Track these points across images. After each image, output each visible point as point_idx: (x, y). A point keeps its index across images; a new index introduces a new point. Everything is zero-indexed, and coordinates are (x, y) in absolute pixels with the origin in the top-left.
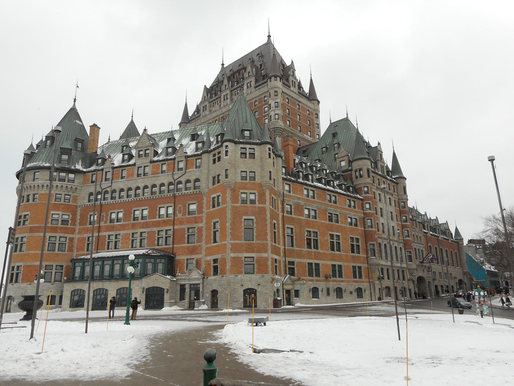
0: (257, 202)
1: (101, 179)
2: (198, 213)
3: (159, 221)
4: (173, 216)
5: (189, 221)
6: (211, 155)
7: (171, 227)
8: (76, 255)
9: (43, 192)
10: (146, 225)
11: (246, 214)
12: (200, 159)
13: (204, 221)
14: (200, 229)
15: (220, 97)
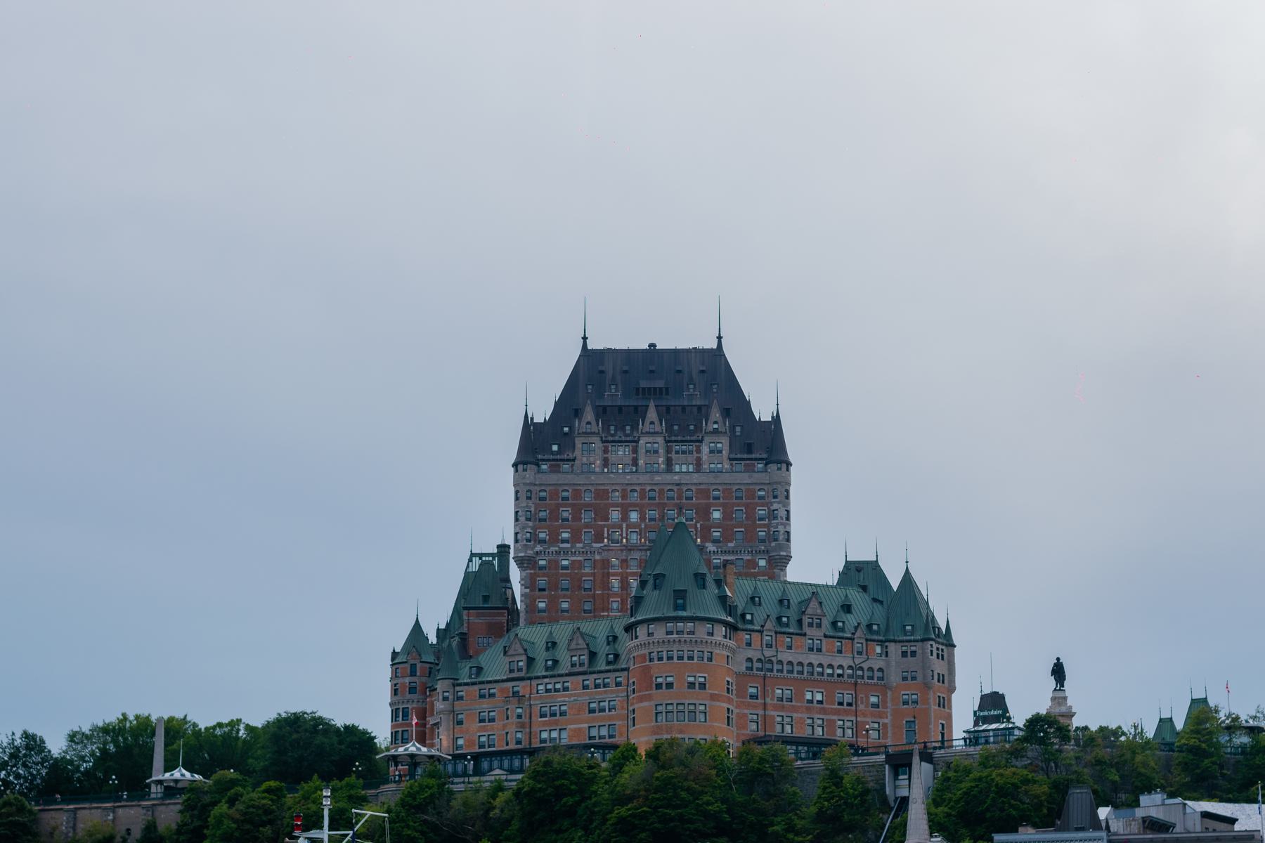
0: (946, 707)
1: (760, 643)
2: (883, 708)
3: (839, 710)
4: (854, 706)
5: (873, 715)
6: (899, 645)
7: (853, 718)
8: (737, 733)
9: (718, 651)
10: (824, 711)
11: (941, 718)
12: (881, 645)
13: (889, 717)
14: (885, 725)
15: (637, 442)
